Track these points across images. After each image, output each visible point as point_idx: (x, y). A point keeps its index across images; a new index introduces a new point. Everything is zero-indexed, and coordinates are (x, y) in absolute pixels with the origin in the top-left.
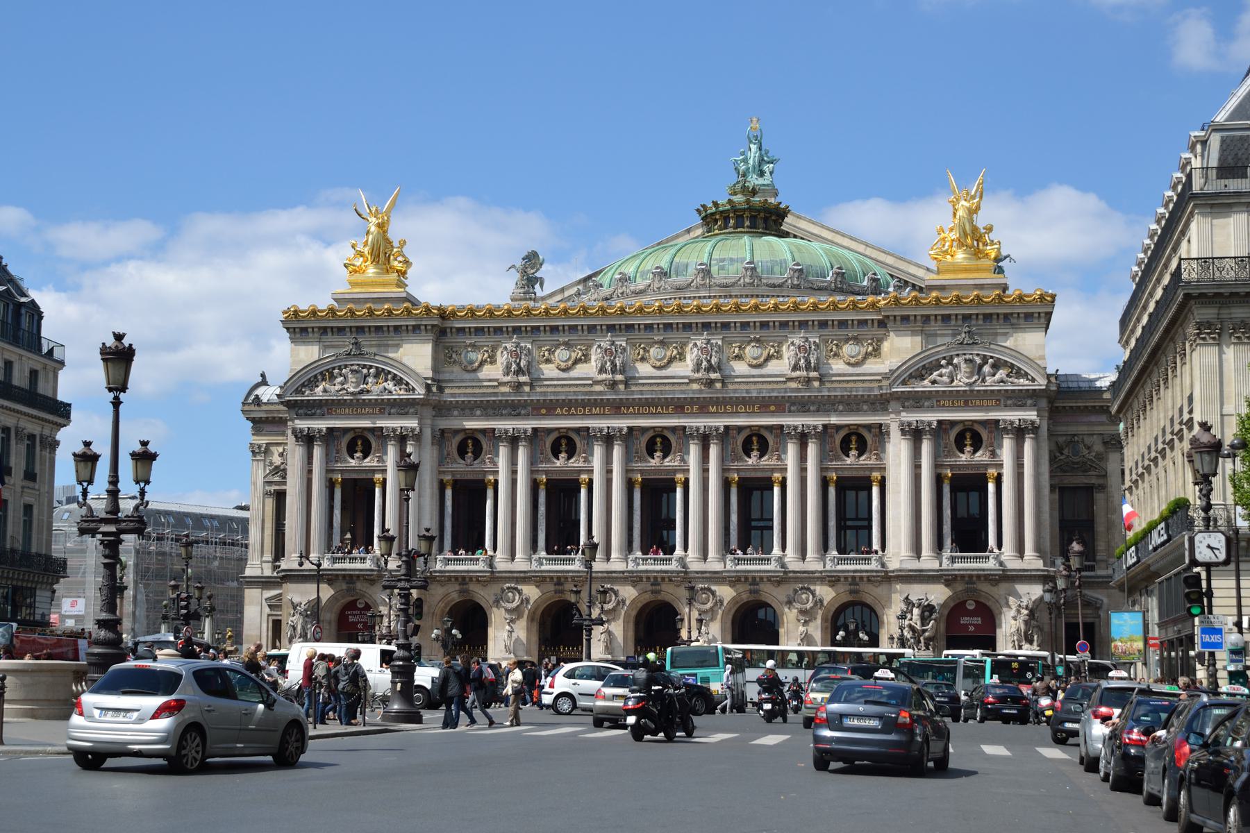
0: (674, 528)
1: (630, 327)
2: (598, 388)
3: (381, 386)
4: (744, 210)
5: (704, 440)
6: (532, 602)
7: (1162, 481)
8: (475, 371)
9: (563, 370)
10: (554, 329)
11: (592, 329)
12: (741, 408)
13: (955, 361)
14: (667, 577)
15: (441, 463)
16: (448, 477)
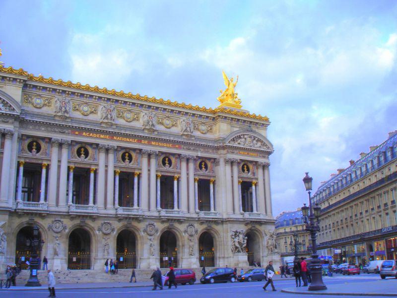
2: (104, 125)
9: (85, 115)
10: (82, 95)
11: (100, 98)
12: (165, 145)
13: (246, 137)
15: (19, 152)
16: (23, 161)
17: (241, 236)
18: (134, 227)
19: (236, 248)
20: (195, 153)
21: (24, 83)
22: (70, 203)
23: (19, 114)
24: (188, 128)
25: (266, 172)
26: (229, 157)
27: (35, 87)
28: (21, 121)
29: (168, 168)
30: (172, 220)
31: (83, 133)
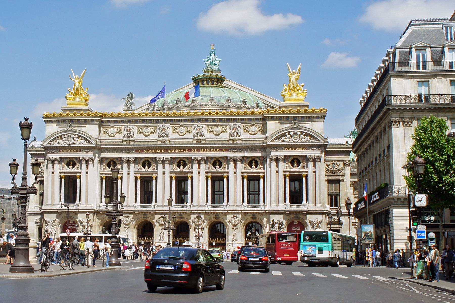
0: (187, 194)
1: (171, 121)
3: (79, 142)
4: (209, 78)
5: (199, 162)
7: (375, 177)
10: (143, 121)
11: (157, 121)
13: (291, 133)
14: (185, 213)
20: (243, 154)
25: (317, 164)
27: (109, 122)
31: (143, 150)
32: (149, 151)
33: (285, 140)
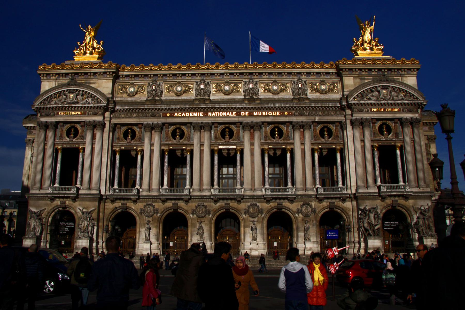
2: (197, 102)
6: (160, 212)
8: (134, 96)
10: (174, 75)
16: (118, 149)
17: (372, 216)
18: (233, 208)
19: (366, 230)
21: (114, 75)
22: (165, 186)
23: (105, 105)
24: (301, 90)
26: (355, 117)
28: (113, 111)
29: (277, 139)
30: (280, 199)
31: (174, 114)
32: (181, 114)
33: (371, 97)
